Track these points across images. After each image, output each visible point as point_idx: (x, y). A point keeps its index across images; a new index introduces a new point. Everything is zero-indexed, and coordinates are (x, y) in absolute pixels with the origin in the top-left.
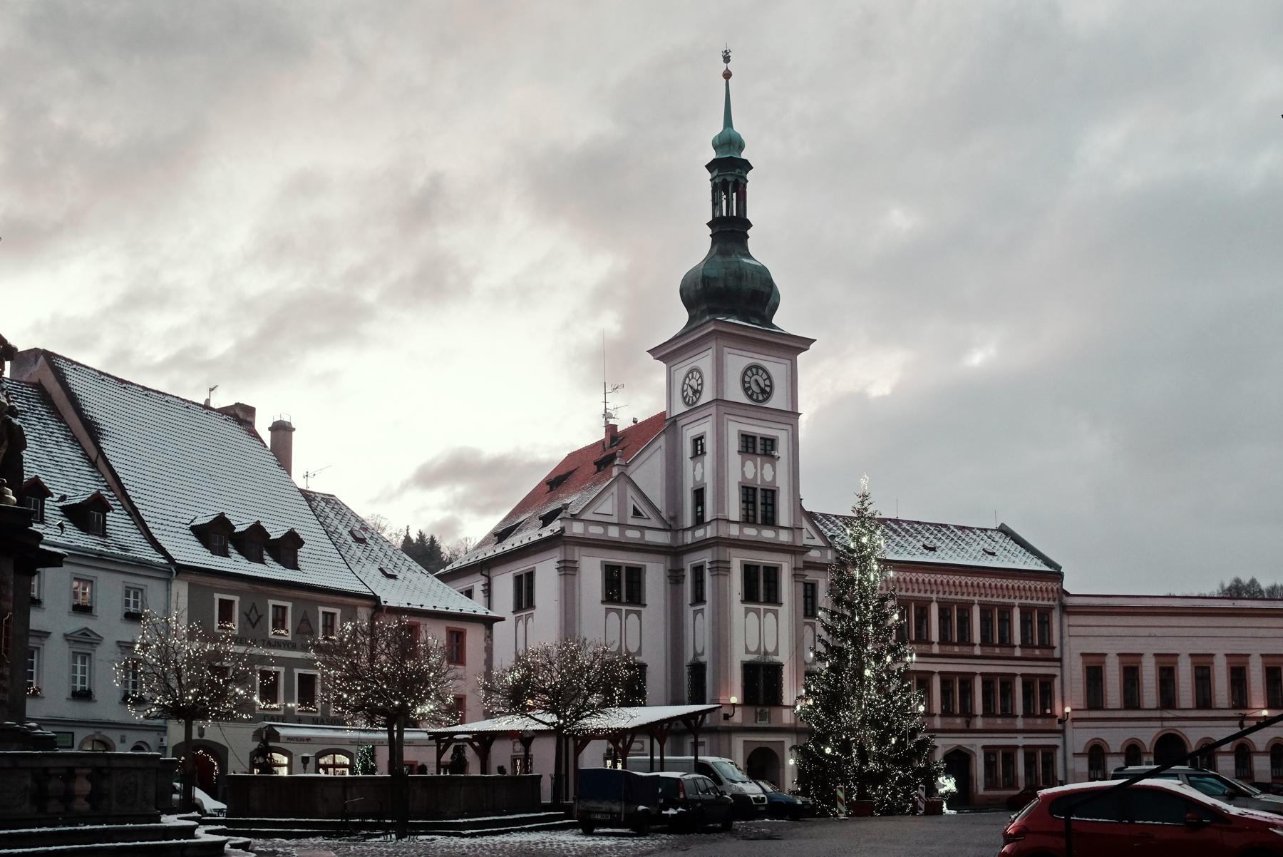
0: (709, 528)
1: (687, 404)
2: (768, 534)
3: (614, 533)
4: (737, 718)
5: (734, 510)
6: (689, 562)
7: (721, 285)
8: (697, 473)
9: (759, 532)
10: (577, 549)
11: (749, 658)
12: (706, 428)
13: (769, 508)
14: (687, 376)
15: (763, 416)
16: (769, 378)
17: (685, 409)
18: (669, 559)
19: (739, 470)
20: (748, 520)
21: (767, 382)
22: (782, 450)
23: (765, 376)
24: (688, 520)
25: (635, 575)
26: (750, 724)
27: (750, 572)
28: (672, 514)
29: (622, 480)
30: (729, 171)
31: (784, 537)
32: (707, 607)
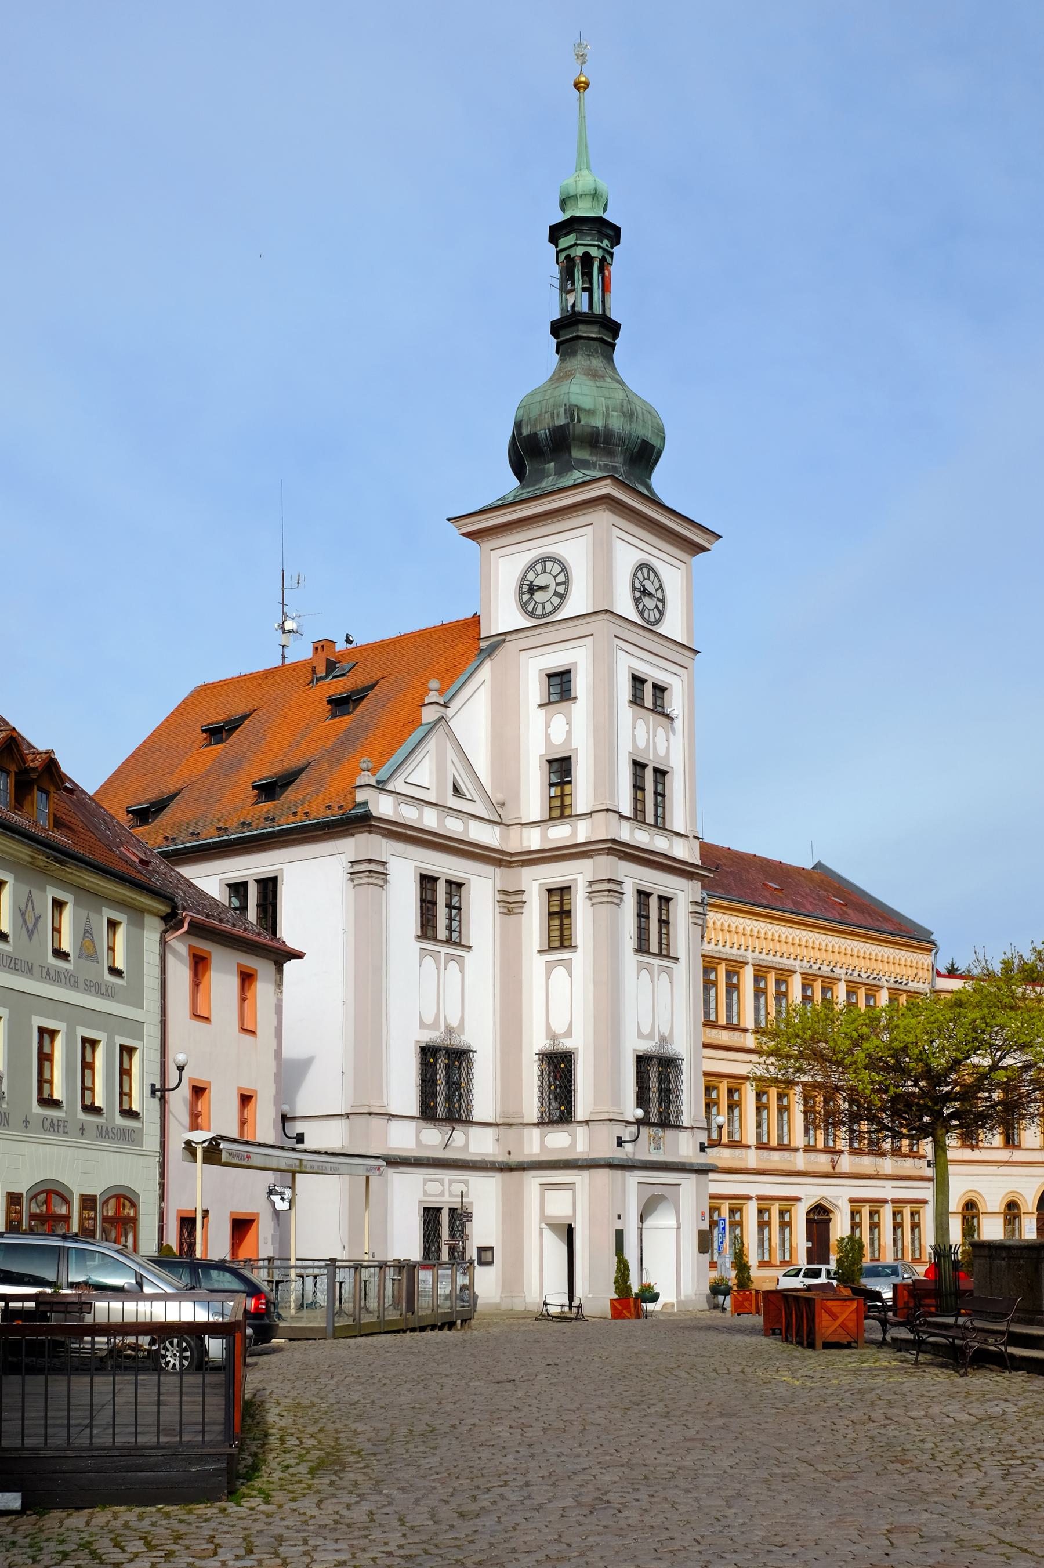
2: (660, 843)
3: (430, 820)
7: (598, 423)
8: (574, 729)
9: (651, 839)
12: (578, 657)
16: (661, 587)
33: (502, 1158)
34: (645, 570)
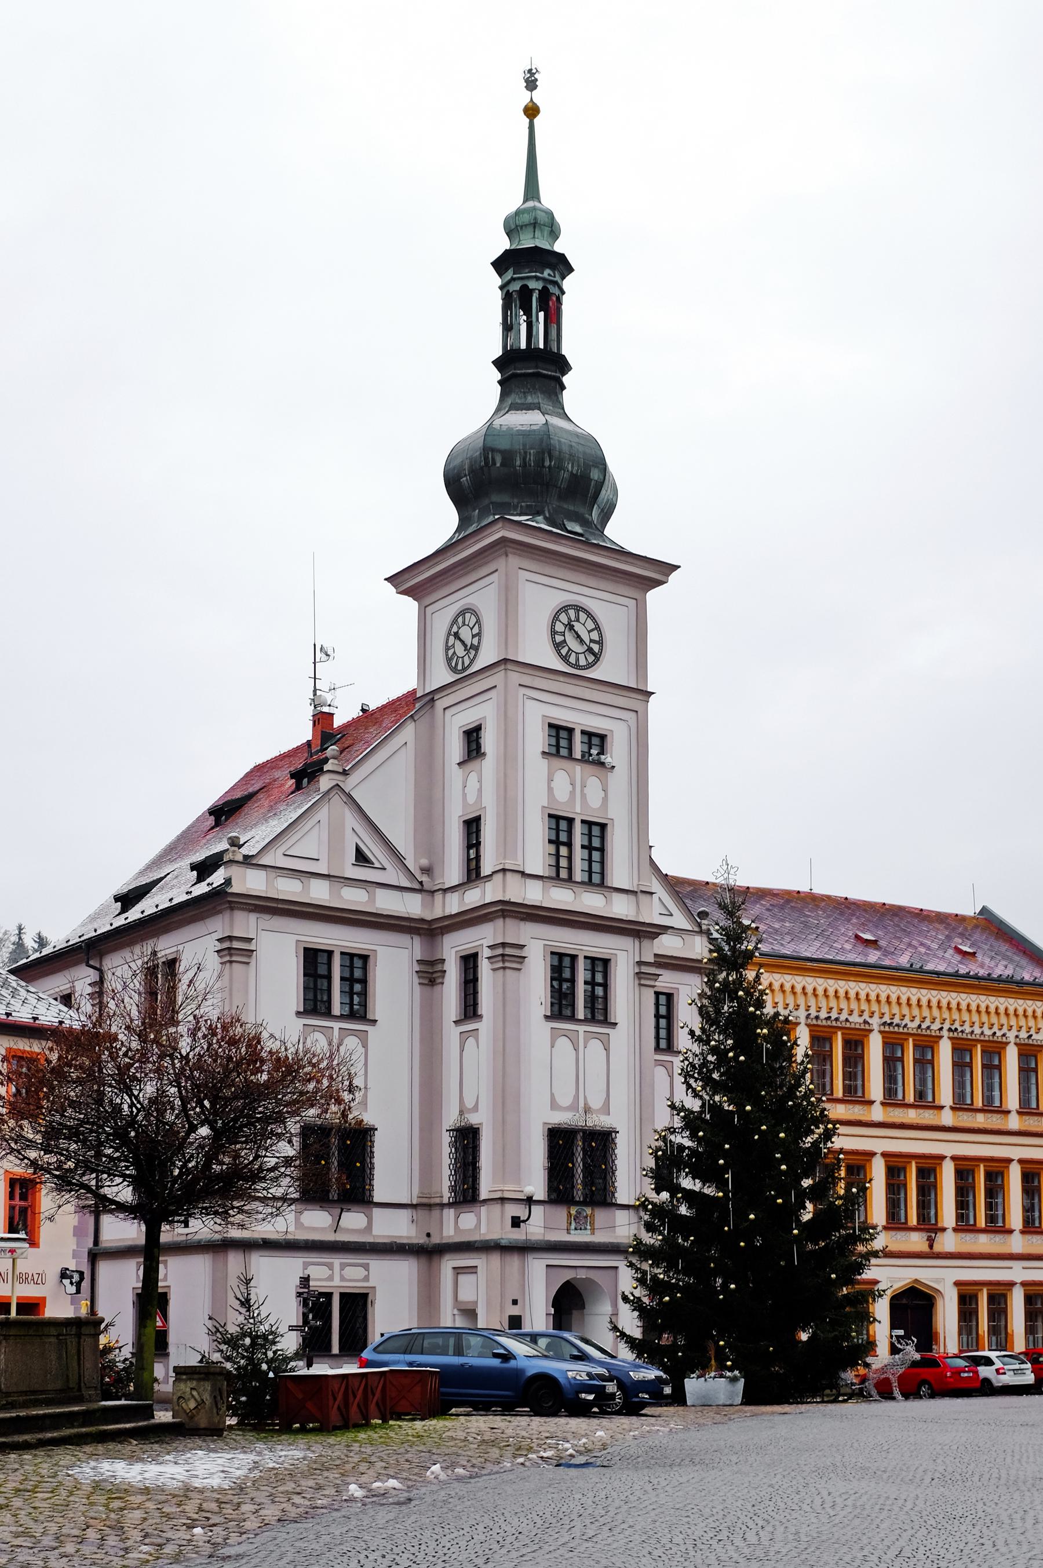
0: (489, 886)
1: (454, 670)
3: (319, 893)
5: (536, 856)
6: (452, 948)
8: (465, 790)
11: (561, 1118)
13: (596, 855)
14: (455, 621)
15: (587, 694)
16: (598, 628)
17: (450, 678)
18: (417, 940)
19: (547, 786)
20: (559, 874)
21: (595, 636)
22: (617, 754)
23: (590, 625)
24: (453, 872)
25: (358, 966)
26: (560, 1236)
27: (561, 966)
28: (424, 862)
29: (337, 799)
30: (532, 270)
32: (485, 1026)
33: (422, 1240)
34: (572, 613)
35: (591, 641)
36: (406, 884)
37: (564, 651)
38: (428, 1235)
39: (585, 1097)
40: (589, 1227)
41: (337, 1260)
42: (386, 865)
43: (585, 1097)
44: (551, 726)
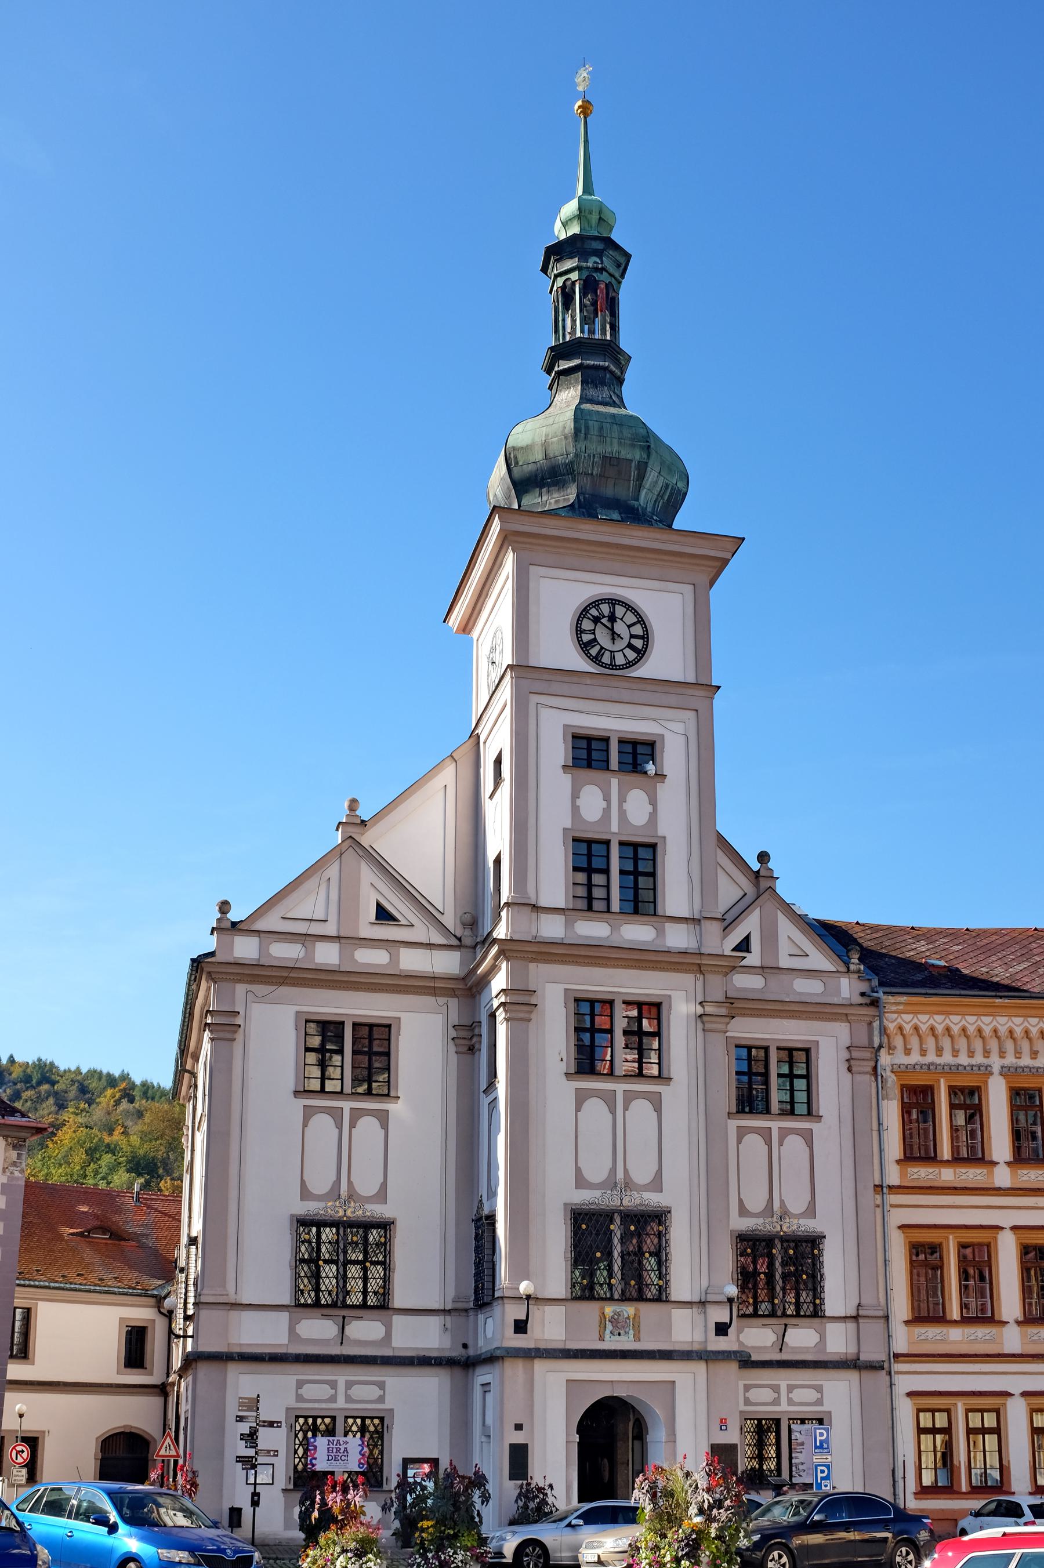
3: (327, 955)
4: (550, 1327)
5: (555, 883)
10: (241, 989)
15: (626, 695)
16: (641, 620)
20: (589, 903)
21: (638, 630)
23: (631, 618)
31: (678, 938)
33: (457, 1352)
34: (605, 609)
35: (632, 636)
36: (442, 941)
37: (594, 652)
38: (465, 1346)
39: (626, 1171)
40: (631, 1332)
41: (342, 1375)
42: (414, 920)
43: (626, 1171)
44: (575, 737)
